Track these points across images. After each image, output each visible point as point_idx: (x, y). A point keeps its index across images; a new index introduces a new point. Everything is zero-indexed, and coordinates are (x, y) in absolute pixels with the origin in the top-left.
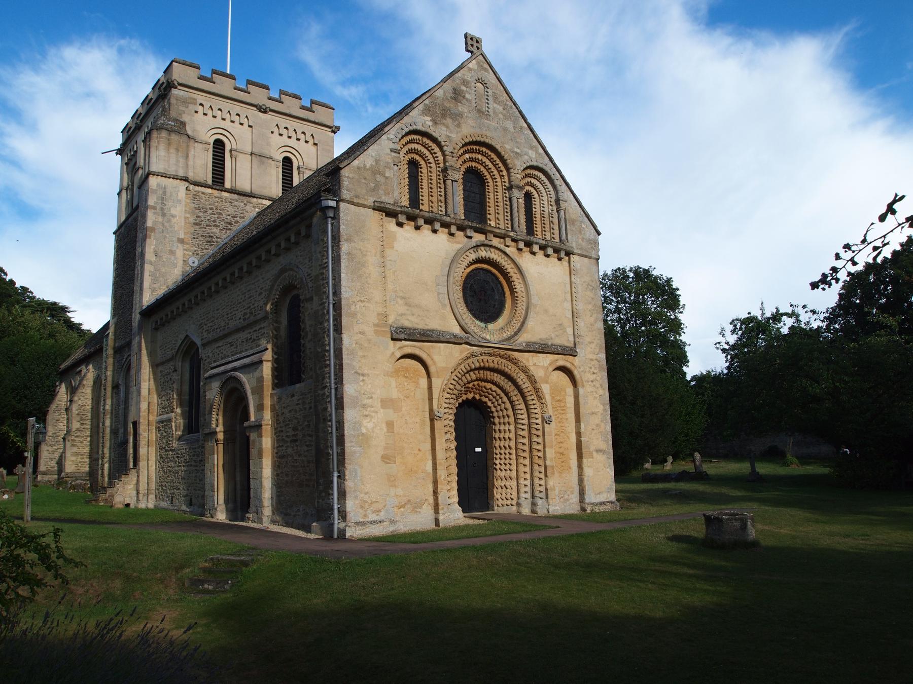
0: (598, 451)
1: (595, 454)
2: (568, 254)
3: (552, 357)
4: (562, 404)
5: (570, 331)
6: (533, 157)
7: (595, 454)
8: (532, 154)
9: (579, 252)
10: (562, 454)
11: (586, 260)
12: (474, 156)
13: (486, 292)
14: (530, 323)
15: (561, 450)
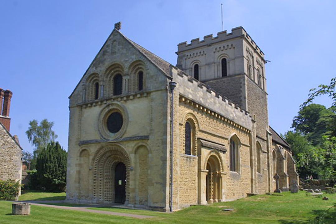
0: (156, 183)
1: (155, 184)
2: (149, 93)
3: (136, 142)
4: (145, 162)
5: (148, 128)
6: (134, 58)
7: (155, 184)
8: (134, 57)
9: (154, 90)
10: (143, 184)
11: (160, 92)
12: (115, 70)
13: (115, 121)
14: (128, 130)
15: (142, 182)
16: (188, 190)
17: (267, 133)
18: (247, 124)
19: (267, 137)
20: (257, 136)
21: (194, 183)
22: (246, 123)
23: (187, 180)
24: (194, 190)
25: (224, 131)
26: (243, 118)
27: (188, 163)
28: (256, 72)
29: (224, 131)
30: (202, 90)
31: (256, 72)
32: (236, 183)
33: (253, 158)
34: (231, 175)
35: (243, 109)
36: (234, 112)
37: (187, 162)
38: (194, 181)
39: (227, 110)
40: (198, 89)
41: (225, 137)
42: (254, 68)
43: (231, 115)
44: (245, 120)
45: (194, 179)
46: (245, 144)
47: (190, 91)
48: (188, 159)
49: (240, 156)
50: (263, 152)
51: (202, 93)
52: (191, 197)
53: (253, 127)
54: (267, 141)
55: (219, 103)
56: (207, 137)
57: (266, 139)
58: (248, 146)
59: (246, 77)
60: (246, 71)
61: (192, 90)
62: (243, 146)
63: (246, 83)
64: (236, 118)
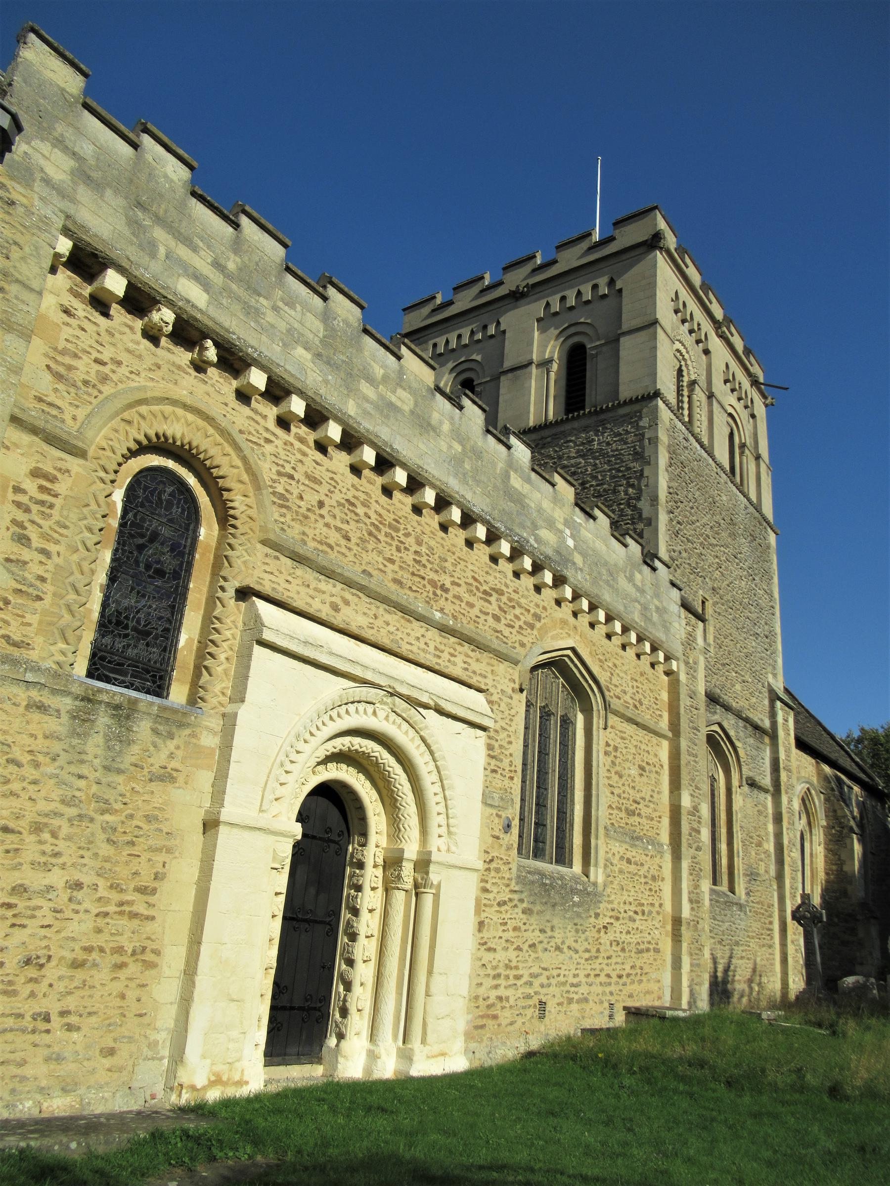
16: (51, 972)
17: (774, 697)
18: (655, 617)
19: (773, 715)
20: (712, 699)
21: (141, 908)
22: (645, 608)
23: (57, 878)
24: (133, 968)
25: (493, 608)
26: (631, 579)
27: (95, 745)
28: (720, 419)
29: (493, 608)
30: (318, 301)
31: (720, 419)
32: (564, 933)
33: (686, 801)
34: (520, 879)
35: (631, 521)
36: (568, 523)
37: (74, 733)
38: (142, 890)
39: (518, 499)
40: (281, 283)
41: (496, 644)
42: (711, 396)
43: (544, 533)
44: (642, 591)
45: (146, 879)
46: (646, 717)
47: (202, 263)
48: (103, 719)
49: (603, 781)
50: (752, 784)
51: (318, 326)
52: (70, 1028)
53: (690, 640)
54: (773, 736)
55: (458, 435)
56: (335, 608)
57: (767, 724)
58: (664, 736)
59: (665, 414)
60: (666, 383)
61: (218, 265)
62: (630, 729)
63: (663, 437)
64: (578, 559)
